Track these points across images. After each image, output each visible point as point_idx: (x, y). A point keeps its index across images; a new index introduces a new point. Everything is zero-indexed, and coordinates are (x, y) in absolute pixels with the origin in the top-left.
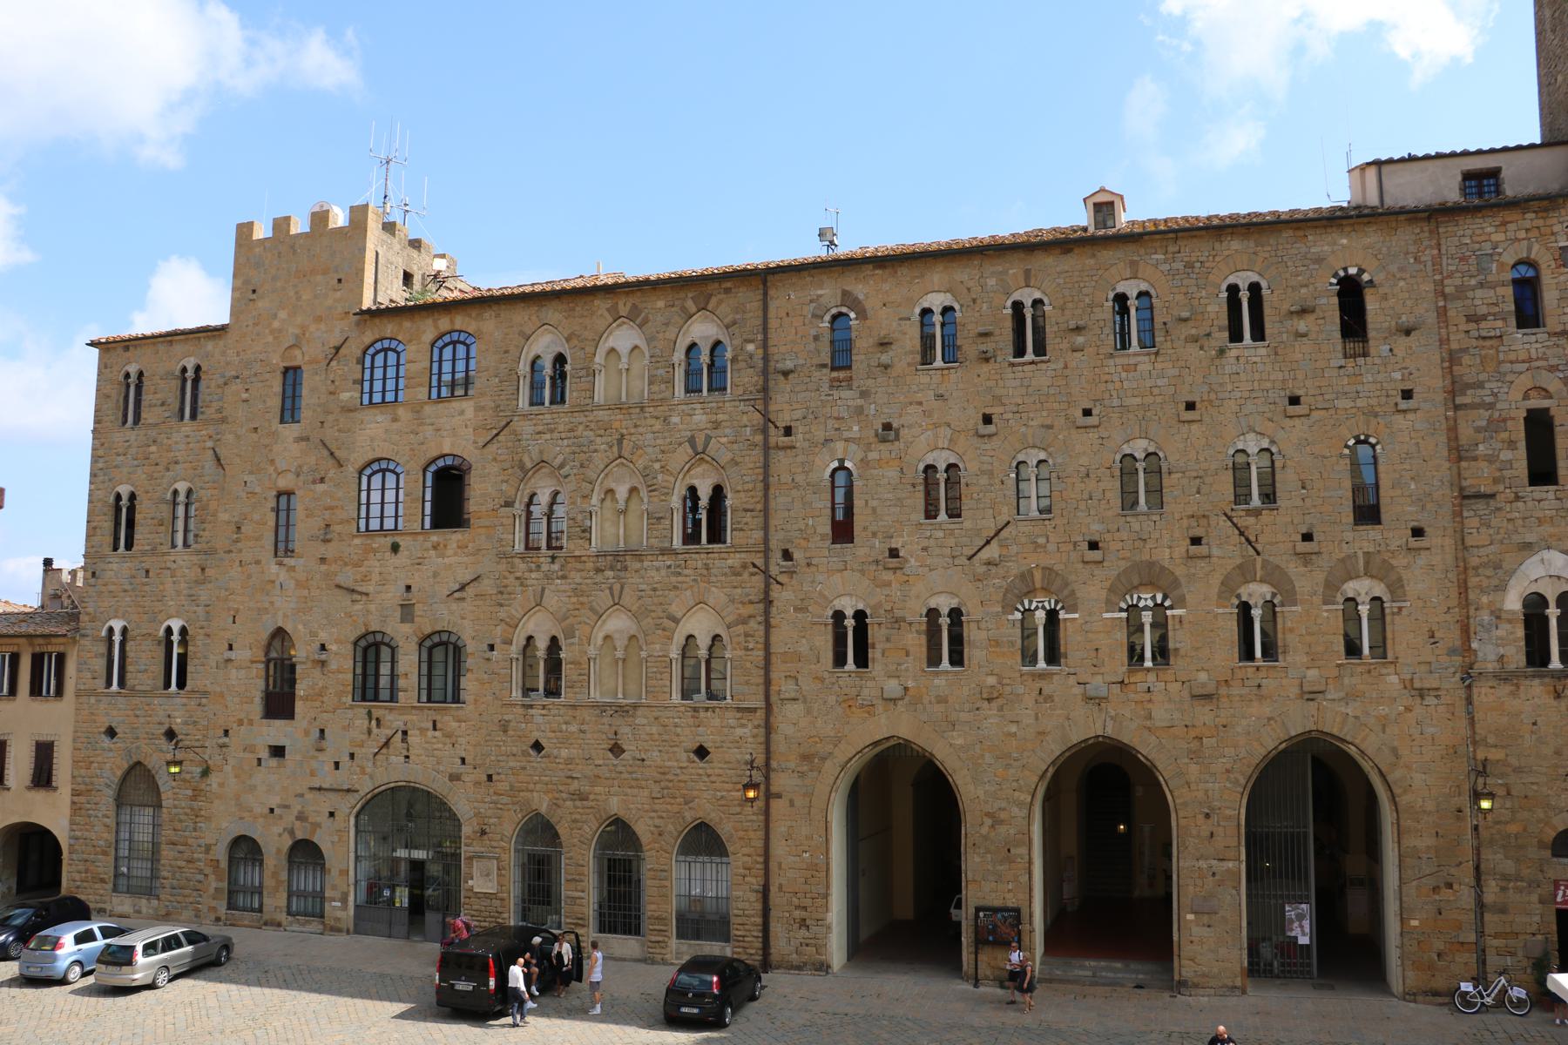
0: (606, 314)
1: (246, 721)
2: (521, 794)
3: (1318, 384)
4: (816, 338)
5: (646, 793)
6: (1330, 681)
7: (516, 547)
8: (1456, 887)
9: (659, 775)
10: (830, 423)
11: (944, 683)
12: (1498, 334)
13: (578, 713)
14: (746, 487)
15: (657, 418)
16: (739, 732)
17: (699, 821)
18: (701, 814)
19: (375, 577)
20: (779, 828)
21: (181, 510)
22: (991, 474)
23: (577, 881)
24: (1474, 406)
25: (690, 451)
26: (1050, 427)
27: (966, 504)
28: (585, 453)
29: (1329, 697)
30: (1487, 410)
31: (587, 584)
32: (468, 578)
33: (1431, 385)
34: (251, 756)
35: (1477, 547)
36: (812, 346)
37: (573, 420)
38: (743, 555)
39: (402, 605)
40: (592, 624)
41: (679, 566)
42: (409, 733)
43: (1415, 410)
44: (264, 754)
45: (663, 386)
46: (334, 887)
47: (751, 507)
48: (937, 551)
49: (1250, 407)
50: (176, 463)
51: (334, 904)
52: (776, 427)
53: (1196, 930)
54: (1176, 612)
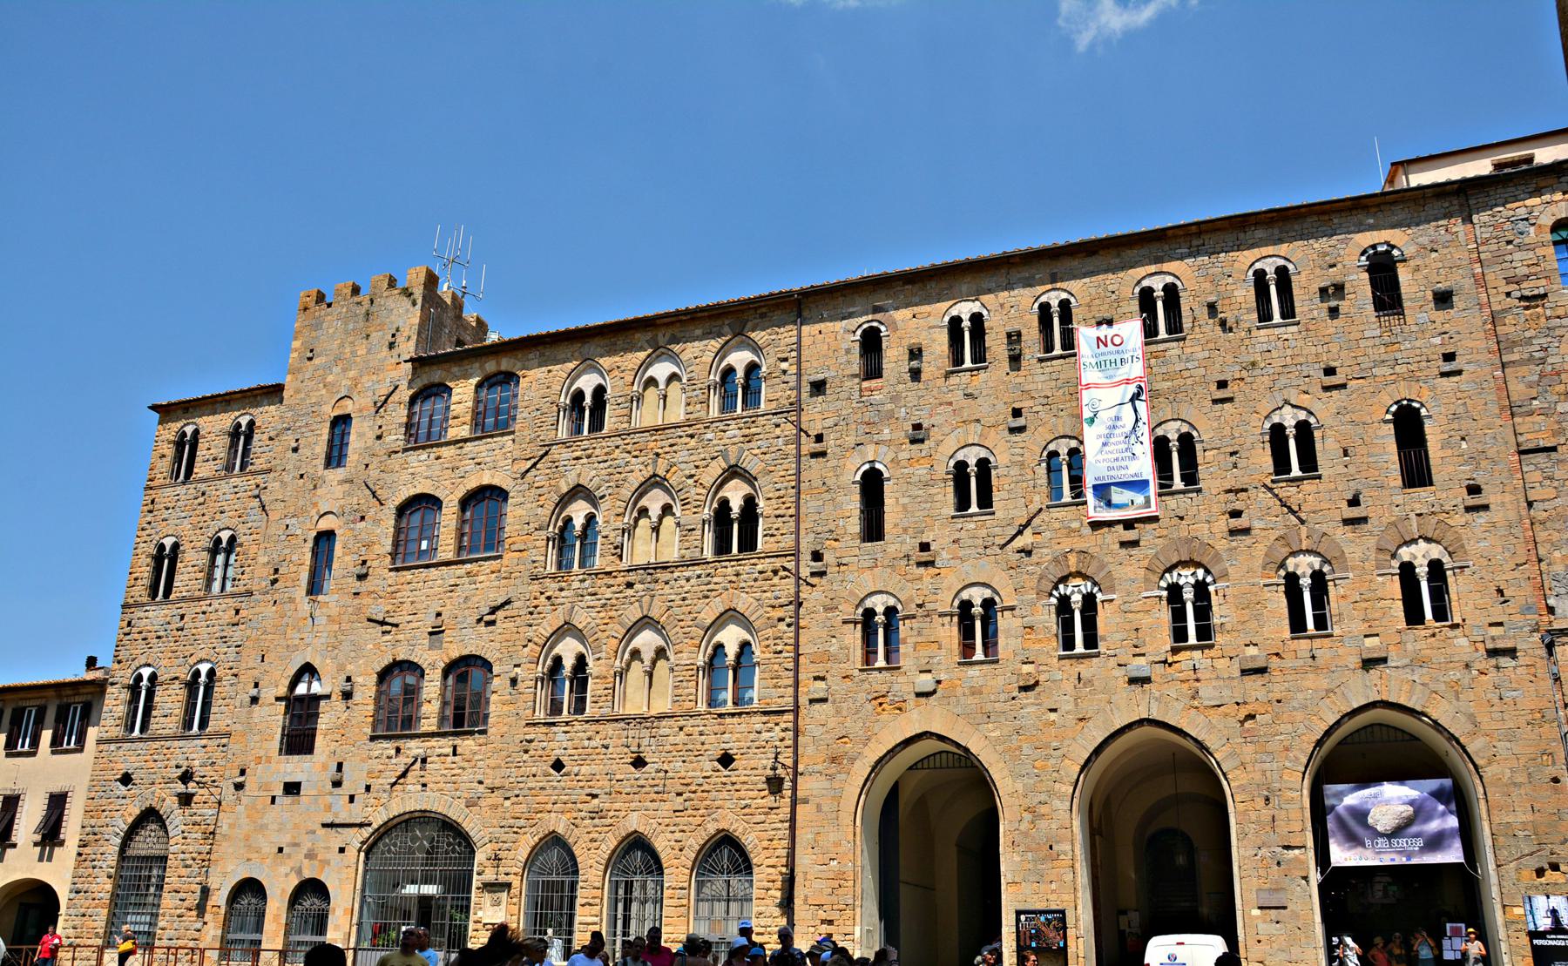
2: (539, 815)
3: (1353, 355)
4: (848, 351)
5: (667, 806)
6: (1391, 647)
7: (548, 568)
9: (682, 787)
11: (978, 673)
12: (1543, 292)
14: (778, 494)
15: (692, 436)
16: (765, 735)
17: (722, 834)
19: (407, 606)
20: (803, 836)
21: (220, 559)
22: (1022, 465)
23: (590, 905)
24: (1521, 363)
27: (996, 496)
28: (620, 473)
29: (1393, 664)
30: (1538, 365)
32: (500, 601)
33: (1474, 348)
34: (265, 793)
35: (1543, 501)
37: (608, 444)
38: (772, 560)
39: (431, 634)
40: (620, 637)
41: (708, 575)
42: (429, 759)
43: (1459, 373)
44: (279, 791)
45: (699, 406)
46: (337, 928)
48: (970, 542)
49: (1283, 380)
50: (222, 512)
52: (808, 436)
53: (1261, 926)
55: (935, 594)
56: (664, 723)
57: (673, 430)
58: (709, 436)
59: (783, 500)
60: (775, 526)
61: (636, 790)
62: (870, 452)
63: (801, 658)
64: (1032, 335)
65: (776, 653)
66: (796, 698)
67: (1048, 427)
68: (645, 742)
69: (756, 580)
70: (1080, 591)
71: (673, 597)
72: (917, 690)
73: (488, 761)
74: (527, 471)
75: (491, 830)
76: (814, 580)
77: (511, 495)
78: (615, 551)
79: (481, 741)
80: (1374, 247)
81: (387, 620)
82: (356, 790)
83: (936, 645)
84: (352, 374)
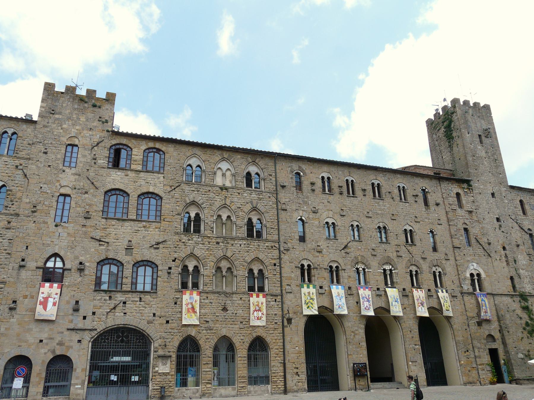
0: (219, 155)
1: (29, 297)
4: (292, 178)
5: (237, 326)
8: (469, 351)
9: (242, 320)
10: (297, 205)
13: (209, 295)
18: (259, 334)
19: (113, 235)
20: (287, 339)
23: (208, 364)
25: (251, 206)
28: (212, 200)
29: (434, 297)
31: (213, 247)
32: (161, 240)
33: (444, 219)
36: (290, 180)
37: (206, 188)
38: (271, 243)
39: (126, 249)
41: (248, 244)
42: (127, 303)
45: (241, 183)
46: (77, 378)
47: (273, 227)
48: (331, 248)
49: (406, 218)
51: (76, 386)
54: (396, 271)
55: (322, 262)
56: (234, 296)
57: (232, 189)
58: (246, 195)
59: (274, 223)
60: (271, 231)
61: (224, 320)
63: (283, 277)
65: (274, 275)
66: (282, 290)
69: (265, 249)
70: (361, 268)
71: (235, 250)
72: (319, 292)
73: (157, 305)
75: (160, 334)
76: (285, 252)
77: (164, 198)
78: (211, 229)
79: (154, 296)
80: (422, 187)
81: (101, 239)
82: (87, 314)
84: (77, 127)
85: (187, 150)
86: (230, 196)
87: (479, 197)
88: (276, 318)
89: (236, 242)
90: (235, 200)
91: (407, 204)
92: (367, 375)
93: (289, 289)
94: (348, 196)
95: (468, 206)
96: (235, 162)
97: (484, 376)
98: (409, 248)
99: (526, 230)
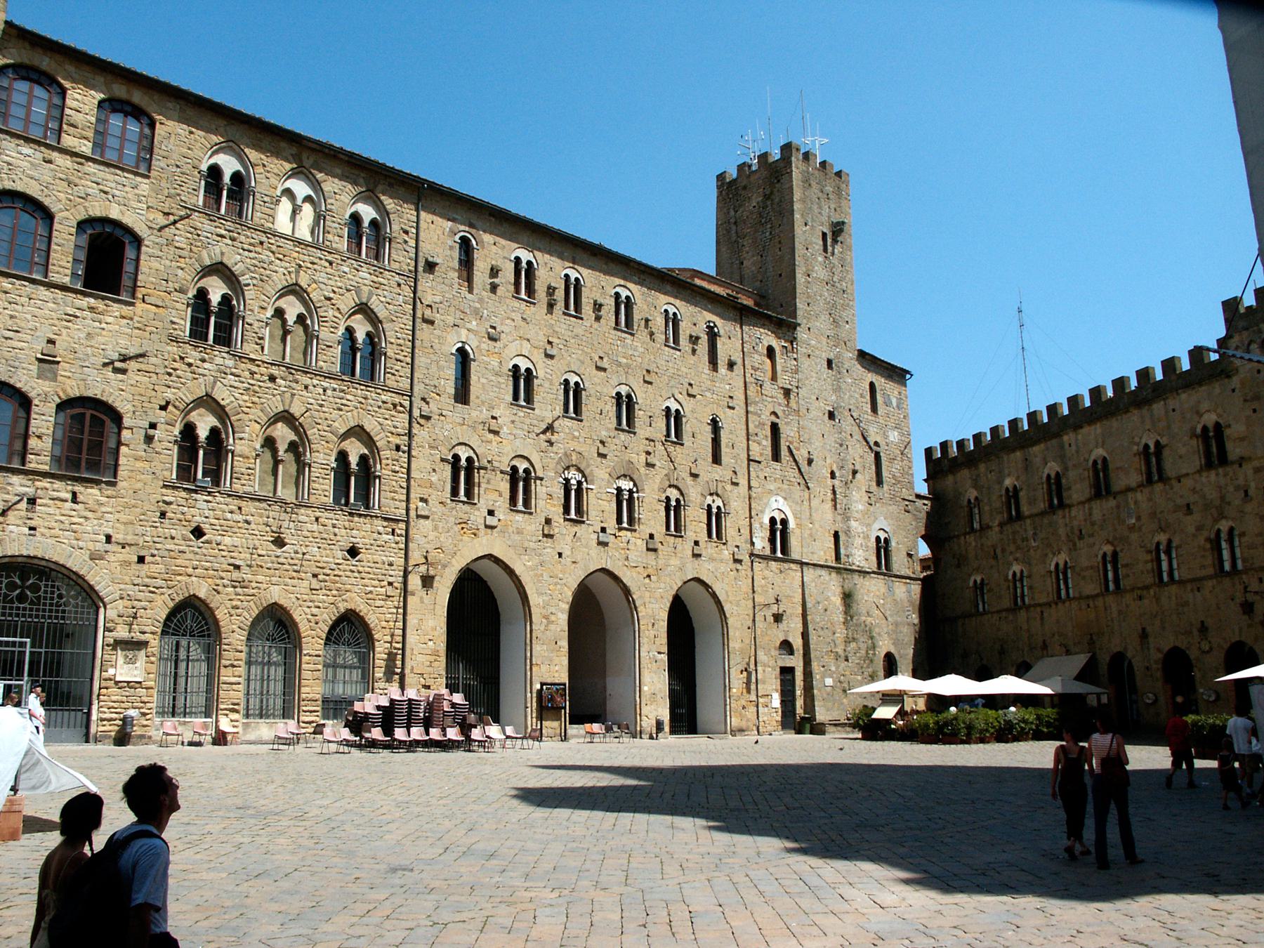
2: (179, 578)
4: (451, 248)
5: (306, 584)
20: (412, 620)
23: (233, 666)
26: (583, 363)
31: (260, 387)
32: (133, 351)
36: (448, 253)
37: (254, 236)
38: (393, 395)
41: (343, 391)
45: (337, 238)
47: (402, 358)
48: (521, 425)
49: (672, 383)
56: (302, 511)
58: (346, 269)
62: (464, 335)
64: (560, 295)
66: (408, 510)
67: (566, 362)
68: (285, 524)
69: (379, 407)
71: (312, 401)
73: (117, 516)
74: (166, 226)
75: (122, 586)
76: (422, 421)
77: (146, 242)
79: (109, 493)
83: (497, 493)
85: (214, 127)
86: (309, 265)
87: (805, 363)
88: (392, 573)
89: (315, 382)
90: (321, 277)
91: (678, 353)
92: (565, 708)
93: (423, 509)
94: (564, 314)
95: (784, 380)
96: (328, 183)
97: (765, 718)
98: (671, 449)
99: (872, 444)
